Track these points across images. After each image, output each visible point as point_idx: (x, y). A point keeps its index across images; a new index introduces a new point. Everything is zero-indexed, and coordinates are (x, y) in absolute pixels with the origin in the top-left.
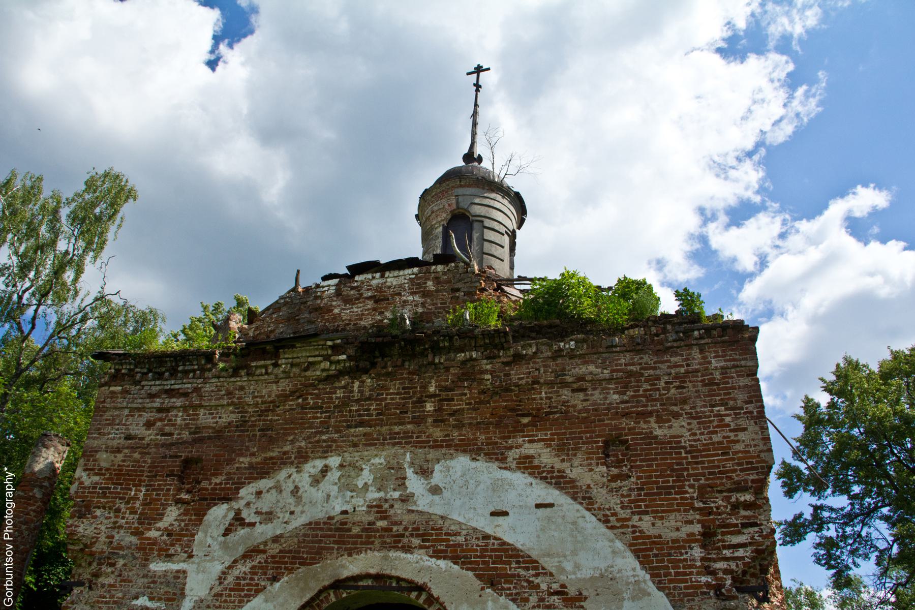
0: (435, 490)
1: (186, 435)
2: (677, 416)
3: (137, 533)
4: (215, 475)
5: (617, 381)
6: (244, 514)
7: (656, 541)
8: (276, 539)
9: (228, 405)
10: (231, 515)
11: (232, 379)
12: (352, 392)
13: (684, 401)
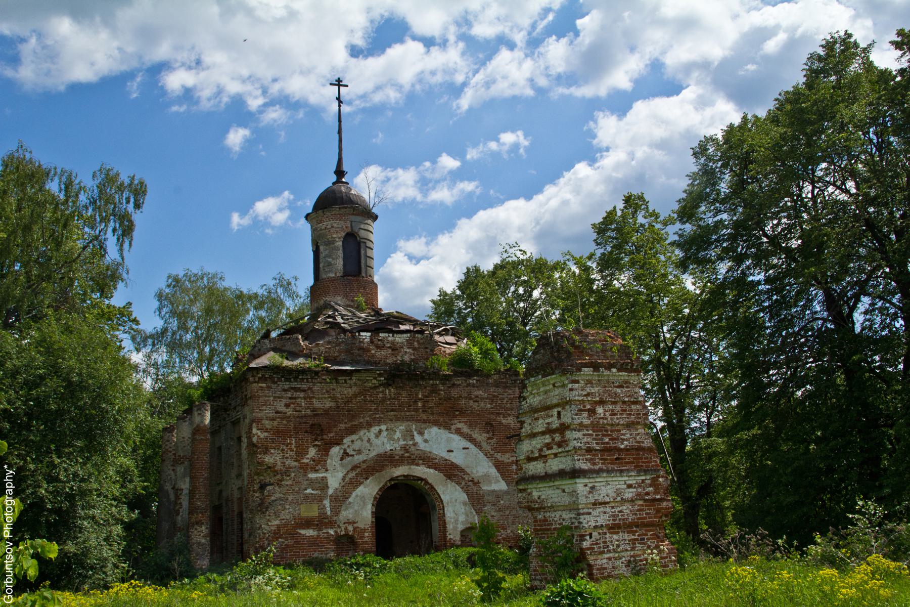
0: (426, 441)
1: (309, 412)
2: (509, 415)
3: (296, 461)
4: (330, 432)
6: (348, 451)
7: (502, 463)
8: (364, 462)
10: (342, 451)
13: (512, 409)
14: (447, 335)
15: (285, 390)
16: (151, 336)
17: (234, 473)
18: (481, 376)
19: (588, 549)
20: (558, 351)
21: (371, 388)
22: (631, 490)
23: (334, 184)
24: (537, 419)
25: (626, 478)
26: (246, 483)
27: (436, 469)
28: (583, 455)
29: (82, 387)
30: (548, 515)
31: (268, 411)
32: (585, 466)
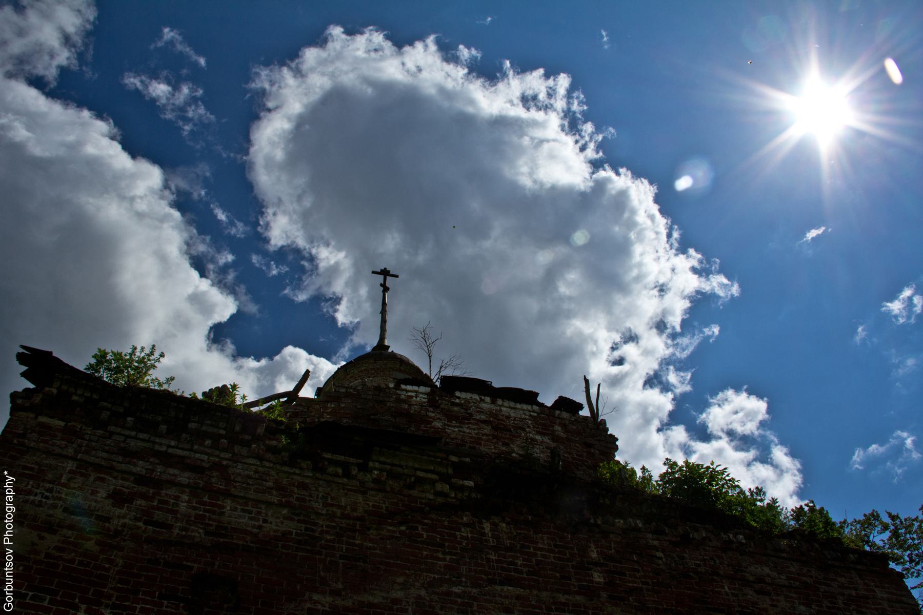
1: (198, 533)
9: (281, 505)
11: (286, 469)
12: (484, 534)
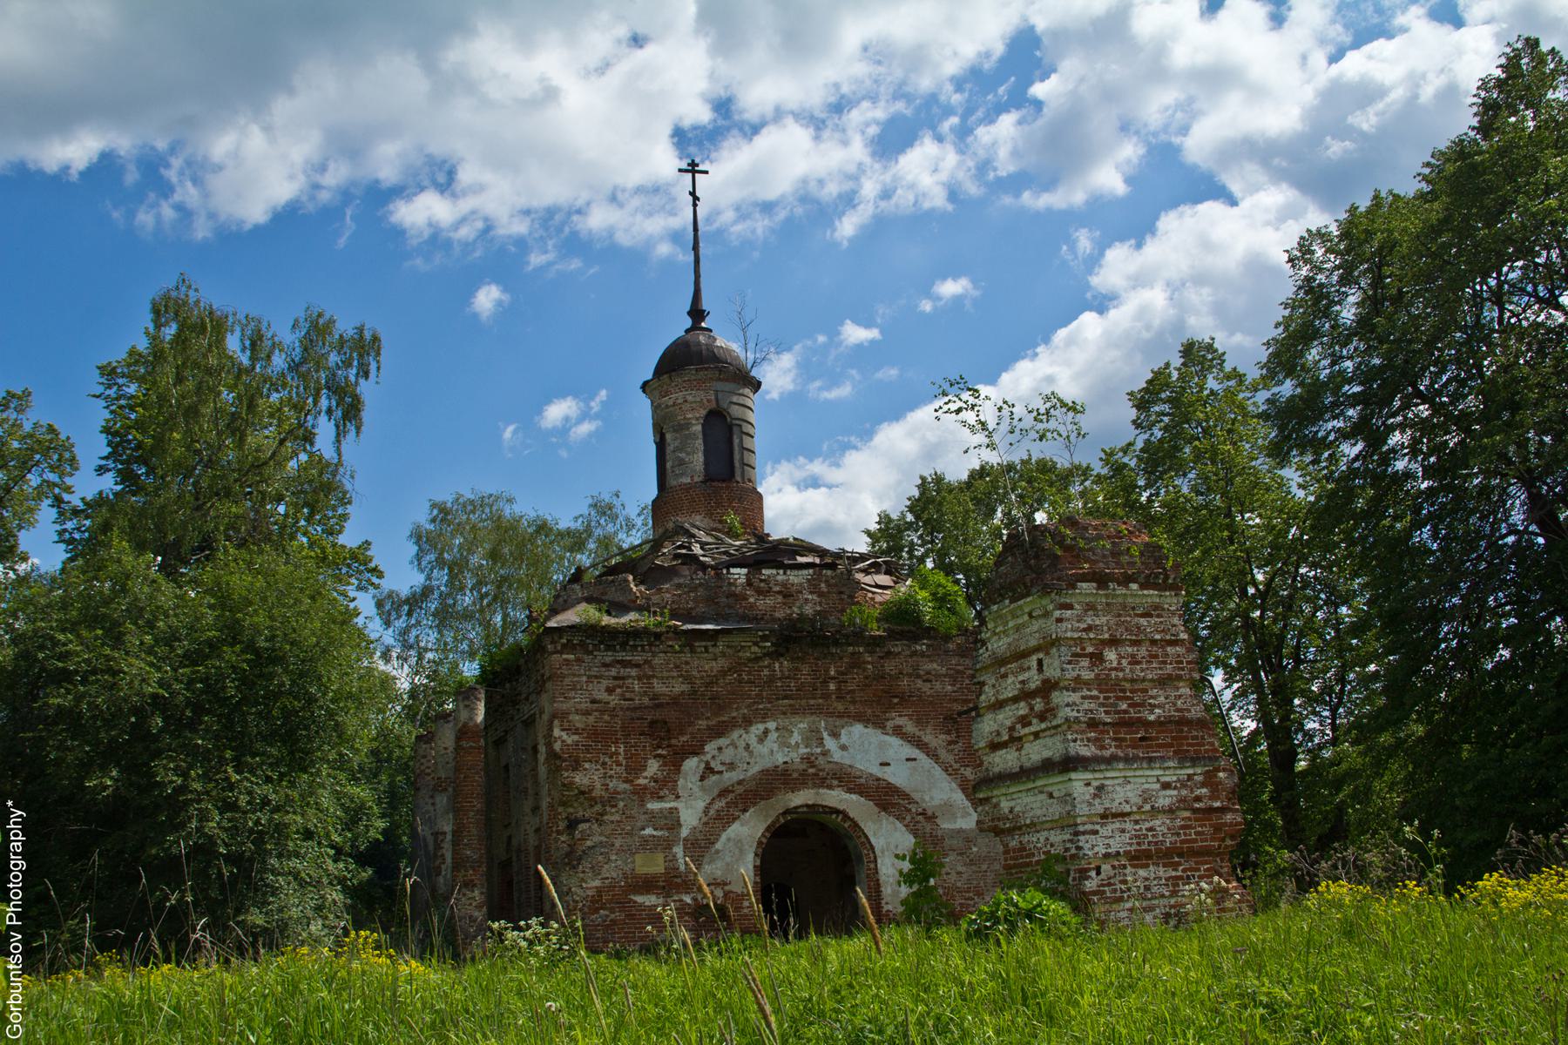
0: (844, 748)
1: (646, 701)
5: (950, 676)
6: (713, 765)
8: (740, 783)
10: (703, 765)
14: (878, 572)
15: (605, 665)
16: (407, 601)
17: (528, 805)
18: (935, 638)
19: (1094, 893)
20: (1037, 557)
21: (750, 660)
22: (1169, 792)
23: (687, 331)
24: (1005, 676)
25: (1160, 772)
26: (545, 820)
27: (861, 794)
28: (1083, 732)
29: (276, 659)
30: (1026, 839)
31: (579, 700)
32: (1086, 751)
